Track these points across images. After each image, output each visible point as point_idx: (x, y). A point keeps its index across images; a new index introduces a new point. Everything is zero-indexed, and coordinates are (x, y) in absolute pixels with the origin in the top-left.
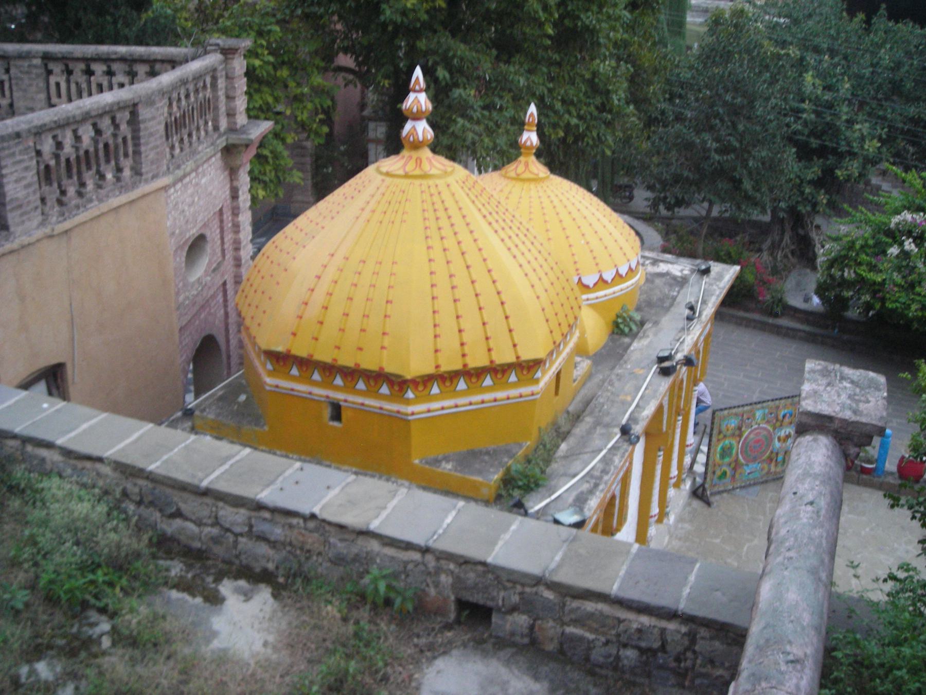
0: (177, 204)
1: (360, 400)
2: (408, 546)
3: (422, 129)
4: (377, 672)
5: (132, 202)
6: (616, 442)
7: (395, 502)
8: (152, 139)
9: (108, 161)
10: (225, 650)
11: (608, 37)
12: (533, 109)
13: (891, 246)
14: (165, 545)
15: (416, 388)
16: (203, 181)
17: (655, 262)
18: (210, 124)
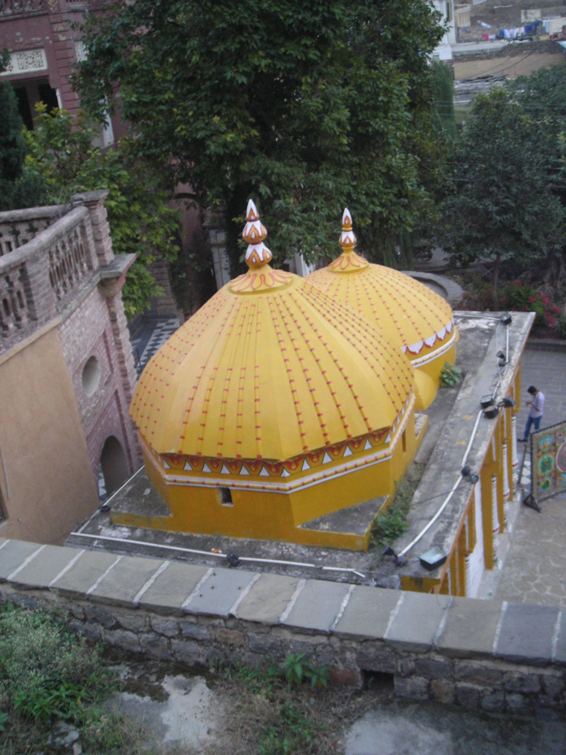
0: (68, 337)
1: (245, 483)
2: (316, 632)
3: (262, 251)
4: (307, 745)
5: (33, 343)
6: (460, 484)
7: (297, 593)
8: (41, 289)
9: (8, 314)
10: (177, 742)
11: (395, 137)
12: (347, 213)
14: (112, 654)
15: (290, 468)
16: (87, 313)
17: (465, 320)
18: (85, 265)
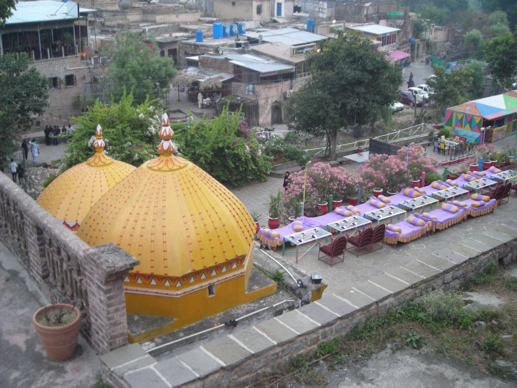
1: (224, 277)
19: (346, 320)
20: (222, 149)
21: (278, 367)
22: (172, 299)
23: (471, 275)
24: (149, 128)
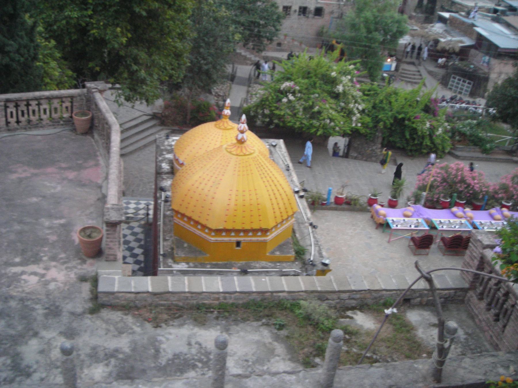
1: (249, 239)
2: (394, 290)
13: (283, 98)
19: (243, 295)
20: (403, 119)
21: (187, 305)
22: (207, 241)
23: (370, 301)
24: (338, 87)
